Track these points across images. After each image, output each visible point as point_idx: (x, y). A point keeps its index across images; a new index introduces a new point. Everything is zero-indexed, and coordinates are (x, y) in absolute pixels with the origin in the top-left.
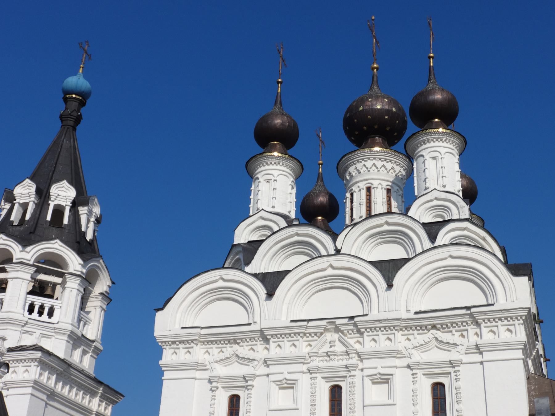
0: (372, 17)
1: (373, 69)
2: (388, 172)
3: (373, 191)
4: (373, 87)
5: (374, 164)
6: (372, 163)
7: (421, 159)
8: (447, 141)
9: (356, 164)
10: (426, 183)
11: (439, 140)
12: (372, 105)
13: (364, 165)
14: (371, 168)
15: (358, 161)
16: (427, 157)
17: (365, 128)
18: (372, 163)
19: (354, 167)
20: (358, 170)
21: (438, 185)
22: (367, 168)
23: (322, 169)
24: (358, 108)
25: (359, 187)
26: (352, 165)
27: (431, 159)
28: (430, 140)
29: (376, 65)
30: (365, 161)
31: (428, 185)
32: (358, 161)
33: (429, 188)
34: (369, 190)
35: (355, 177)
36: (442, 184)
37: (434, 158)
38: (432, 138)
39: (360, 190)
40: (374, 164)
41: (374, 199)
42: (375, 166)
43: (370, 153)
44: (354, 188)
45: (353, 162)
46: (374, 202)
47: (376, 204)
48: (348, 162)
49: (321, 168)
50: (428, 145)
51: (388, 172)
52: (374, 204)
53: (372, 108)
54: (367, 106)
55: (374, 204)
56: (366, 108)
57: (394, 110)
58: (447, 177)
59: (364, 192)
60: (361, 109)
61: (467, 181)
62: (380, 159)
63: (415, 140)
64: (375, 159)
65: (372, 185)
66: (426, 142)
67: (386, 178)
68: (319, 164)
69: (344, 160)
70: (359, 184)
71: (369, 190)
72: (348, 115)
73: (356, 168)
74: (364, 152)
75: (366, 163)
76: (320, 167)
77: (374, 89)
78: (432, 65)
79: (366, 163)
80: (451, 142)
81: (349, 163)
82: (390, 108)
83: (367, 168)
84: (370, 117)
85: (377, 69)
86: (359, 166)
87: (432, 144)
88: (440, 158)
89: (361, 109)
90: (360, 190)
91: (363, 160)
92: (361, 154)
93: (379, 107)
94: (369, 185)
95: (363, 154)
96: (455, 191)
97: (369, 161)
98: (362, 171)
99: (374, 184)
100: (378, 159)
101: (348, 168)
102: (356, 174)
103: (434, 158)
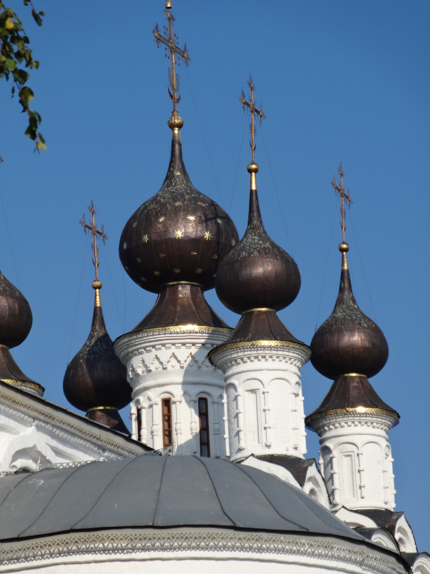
0: (166, 4)
1: (172, 126)
2: (199, 367)
3: (173, 407)
4: (173, 171)
5: (174, 356)
6: (169, 353)
7: (232, 390)
8: (274, 358)
9: (141, 353)
10: (239, 440)
11: (260, 358)
12: (166, 231)
13: (157, 357)
14: (168, 362)
15: (145, 348)
16: (241, 390)
17: (157, 273)
18: (169, 353)
19: (139, 357)
20: (146, 366)
21: (259, 443)
22: (161, 363)
23: (100, 298)
24: (140, 237)
25: (149, 399)
26: (135, 355)
27: (247, 393)
28: (245, 359)
29: (178, 119)
30: (156, 349)
31: (242, 444)
32: (145, 348)
33: (243, 449)
34: (167, 403)
35: (143, 376)
36: (264, 441)
37: (253, 391)
38: (248, 355)
39: (151, 406)
40: (173, 354)
41: (176, 423)
42: (176, 358)
43: (163, 336)
44: (141, 398)
45: (137, 350)
46: (176, 431)
47: (179, 435)
48: (128, 348)
49: (100, 295)
50: (242, 367)
51: (199, 367)
52: (177, 434)
53: (164, 239)
54: (156, 233)
55: (177, 434)
56: (154, 237)
57: (207, 235)
58: (273, 428)
59: (158, 410)
60: (146, 238)
61: (363, 337)
62: (184, 344)
63: (221, 357)
64: (174, 344)
65: (172, 397)
66: (239, 361)
67: (195, 380)
68: (95, 288)
69: (123, 344)
70: (150, 393)
71: (167, 403)
72: (125, 246)
73: (143, 361)
74: (153, 335)
75: (158, 353)
76: (96, 295)
77: (173, 176)
78: (254, 188)
79: (158, 353)
80: (281, 358)
81: (130, 350)
82: (199, 234)
83: (161, 363)
84: (162, 255)
85: (180, 126)
86: (148, 357)
87: (249, 366)
88: (261, 392)
89: (146, 238)
90: (151, 406)
91: (154, 347)
92: (148, 338)
93: (179, 234)
94: (167, 396)
95: (151, 337)
96: (287, 450)
97: (163, 348)
98: (152, 368)
99: (175, 395)
100: (181, 345)
101: (131, 358)
102: (143, 372)
103: (253, 391)
